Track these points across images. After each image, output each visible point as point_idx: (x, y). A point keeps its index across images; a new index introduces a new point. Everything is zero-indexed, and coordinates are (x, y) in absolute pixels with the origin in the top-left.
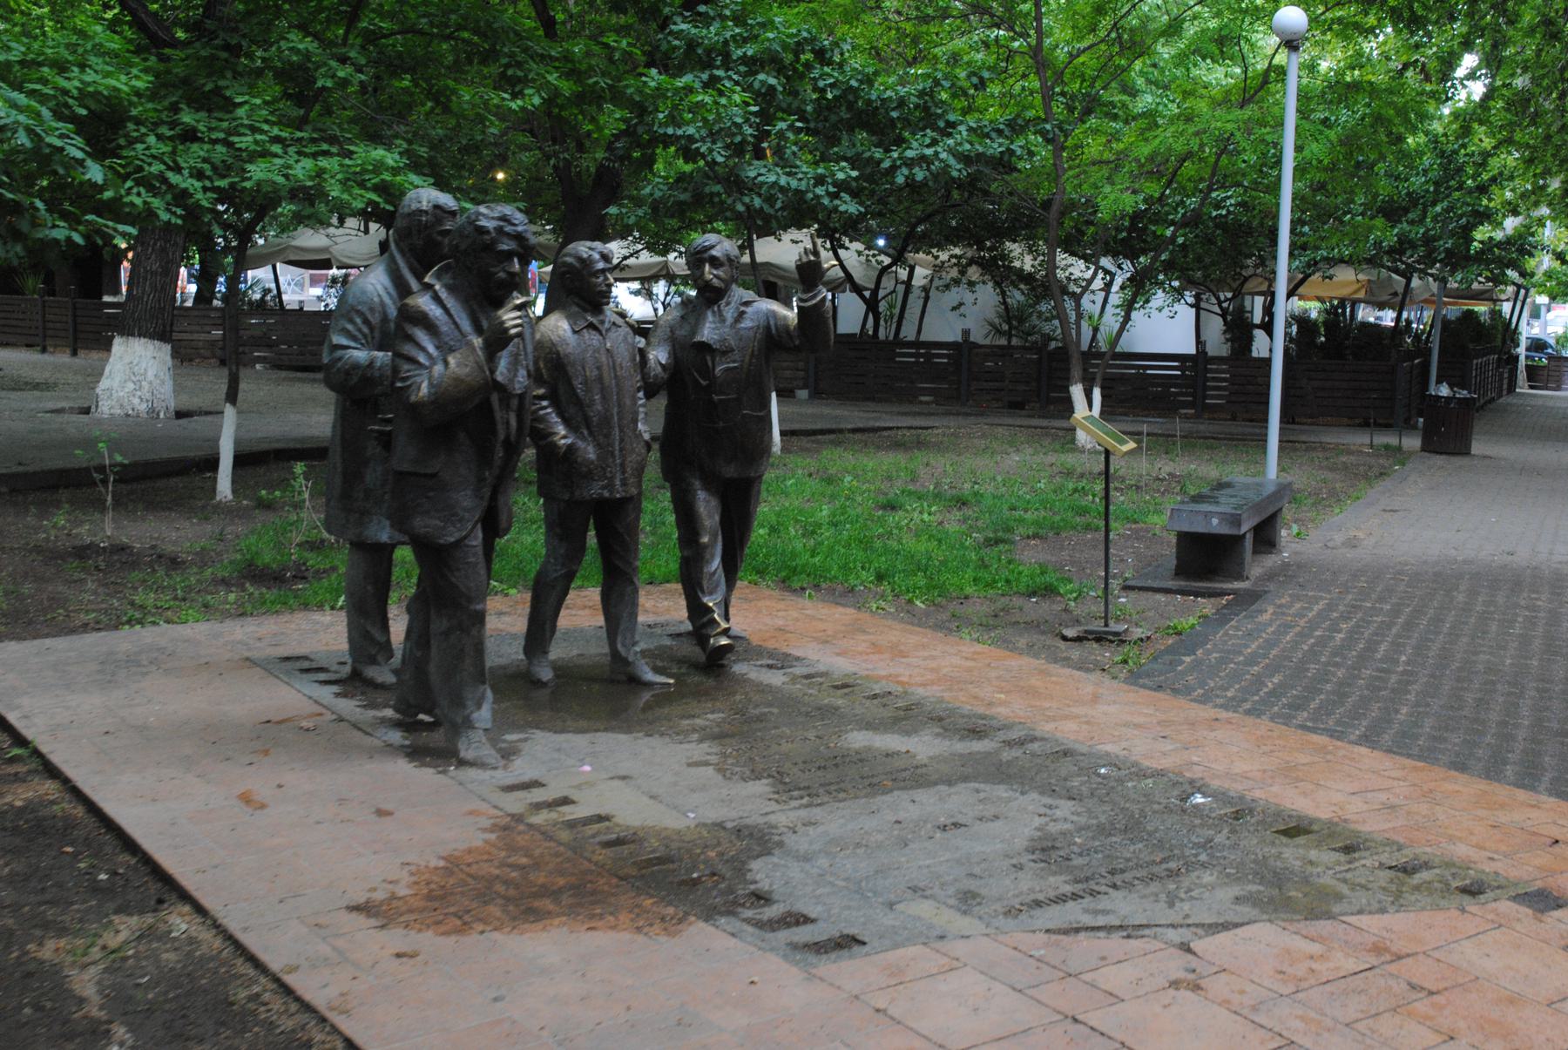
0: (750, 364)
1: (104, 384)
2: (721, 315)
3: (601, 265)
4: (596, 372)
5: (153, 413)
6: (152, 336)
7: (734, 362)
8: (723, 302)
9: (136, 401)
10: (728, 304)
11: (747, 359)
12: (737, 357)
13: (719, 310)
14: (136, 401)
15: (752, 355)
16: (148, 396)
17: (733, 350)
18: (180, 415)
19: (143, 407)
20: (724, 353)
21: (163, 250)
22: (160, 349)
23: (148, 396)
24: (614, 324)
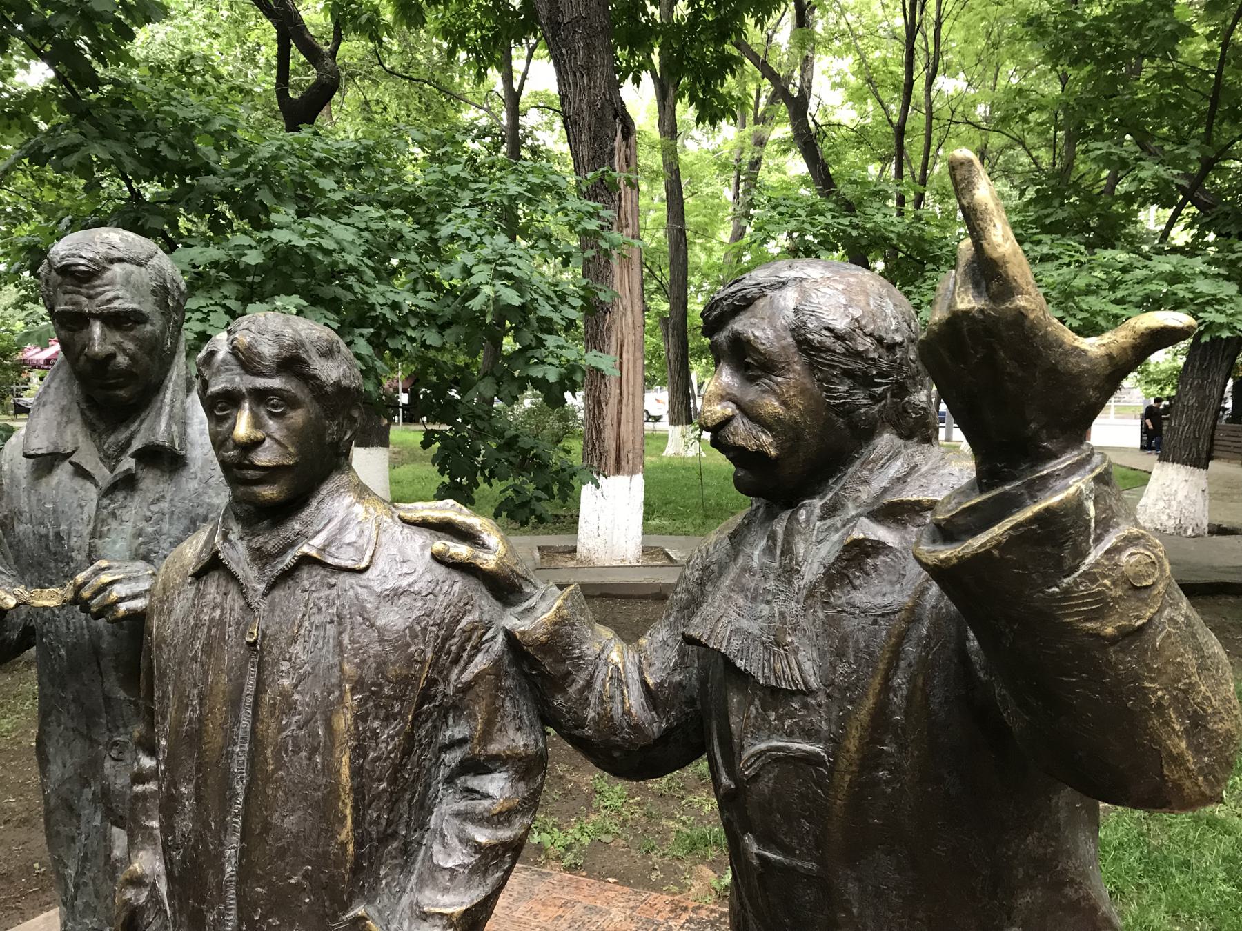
0: (870, 759)
1: (1142, 502)
2: (788, 550)
3: (242, 382)
4: (192, 714)
5: (1180, 527)
6: (1185, 463)
7: (810, 734)
8: (818, 503)
9: (1165, 517)
10: (830, 511)
11: (852, 744)
12: (818, 720)
13: (789, 533)
14: (1165, 517)
15: (880, 719)
16: (1177, 514)
17: (810, 692)
18: (1218, 530)
19: (1171, 523)
20: (776, 696)
21: (1201, 387)
22: (1193, 474)
23: (1177, 514)
24: (305, 560)
